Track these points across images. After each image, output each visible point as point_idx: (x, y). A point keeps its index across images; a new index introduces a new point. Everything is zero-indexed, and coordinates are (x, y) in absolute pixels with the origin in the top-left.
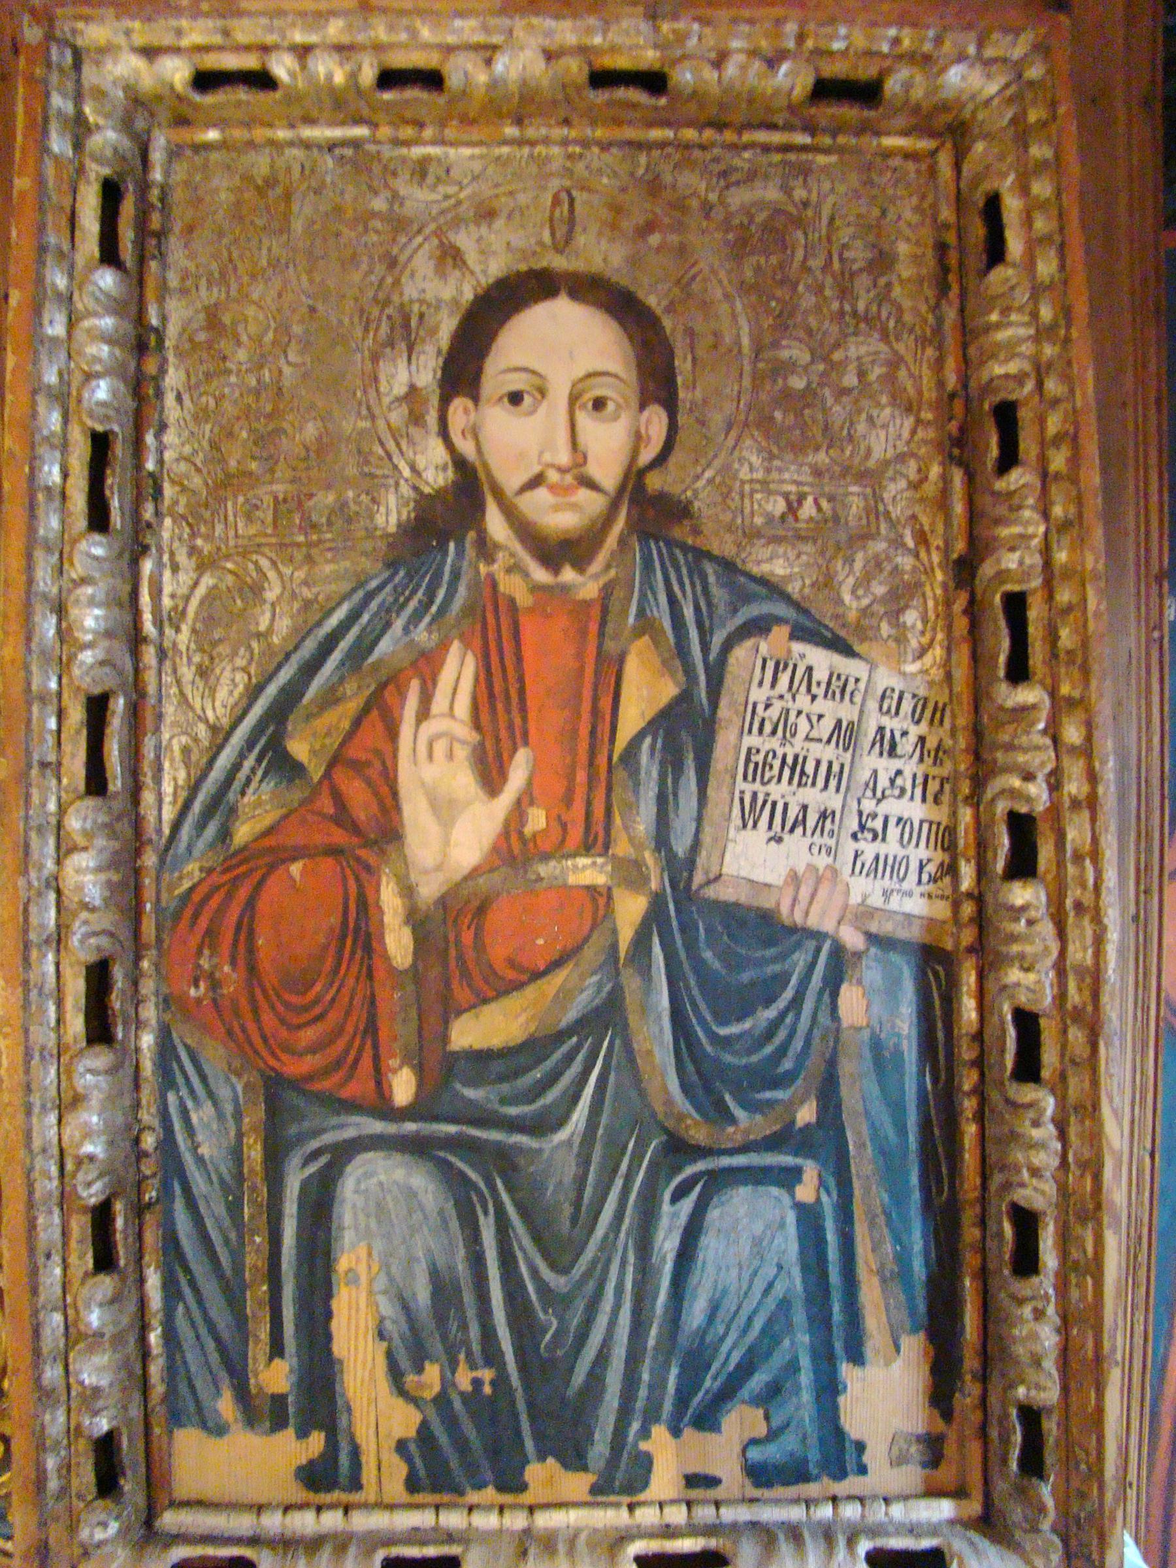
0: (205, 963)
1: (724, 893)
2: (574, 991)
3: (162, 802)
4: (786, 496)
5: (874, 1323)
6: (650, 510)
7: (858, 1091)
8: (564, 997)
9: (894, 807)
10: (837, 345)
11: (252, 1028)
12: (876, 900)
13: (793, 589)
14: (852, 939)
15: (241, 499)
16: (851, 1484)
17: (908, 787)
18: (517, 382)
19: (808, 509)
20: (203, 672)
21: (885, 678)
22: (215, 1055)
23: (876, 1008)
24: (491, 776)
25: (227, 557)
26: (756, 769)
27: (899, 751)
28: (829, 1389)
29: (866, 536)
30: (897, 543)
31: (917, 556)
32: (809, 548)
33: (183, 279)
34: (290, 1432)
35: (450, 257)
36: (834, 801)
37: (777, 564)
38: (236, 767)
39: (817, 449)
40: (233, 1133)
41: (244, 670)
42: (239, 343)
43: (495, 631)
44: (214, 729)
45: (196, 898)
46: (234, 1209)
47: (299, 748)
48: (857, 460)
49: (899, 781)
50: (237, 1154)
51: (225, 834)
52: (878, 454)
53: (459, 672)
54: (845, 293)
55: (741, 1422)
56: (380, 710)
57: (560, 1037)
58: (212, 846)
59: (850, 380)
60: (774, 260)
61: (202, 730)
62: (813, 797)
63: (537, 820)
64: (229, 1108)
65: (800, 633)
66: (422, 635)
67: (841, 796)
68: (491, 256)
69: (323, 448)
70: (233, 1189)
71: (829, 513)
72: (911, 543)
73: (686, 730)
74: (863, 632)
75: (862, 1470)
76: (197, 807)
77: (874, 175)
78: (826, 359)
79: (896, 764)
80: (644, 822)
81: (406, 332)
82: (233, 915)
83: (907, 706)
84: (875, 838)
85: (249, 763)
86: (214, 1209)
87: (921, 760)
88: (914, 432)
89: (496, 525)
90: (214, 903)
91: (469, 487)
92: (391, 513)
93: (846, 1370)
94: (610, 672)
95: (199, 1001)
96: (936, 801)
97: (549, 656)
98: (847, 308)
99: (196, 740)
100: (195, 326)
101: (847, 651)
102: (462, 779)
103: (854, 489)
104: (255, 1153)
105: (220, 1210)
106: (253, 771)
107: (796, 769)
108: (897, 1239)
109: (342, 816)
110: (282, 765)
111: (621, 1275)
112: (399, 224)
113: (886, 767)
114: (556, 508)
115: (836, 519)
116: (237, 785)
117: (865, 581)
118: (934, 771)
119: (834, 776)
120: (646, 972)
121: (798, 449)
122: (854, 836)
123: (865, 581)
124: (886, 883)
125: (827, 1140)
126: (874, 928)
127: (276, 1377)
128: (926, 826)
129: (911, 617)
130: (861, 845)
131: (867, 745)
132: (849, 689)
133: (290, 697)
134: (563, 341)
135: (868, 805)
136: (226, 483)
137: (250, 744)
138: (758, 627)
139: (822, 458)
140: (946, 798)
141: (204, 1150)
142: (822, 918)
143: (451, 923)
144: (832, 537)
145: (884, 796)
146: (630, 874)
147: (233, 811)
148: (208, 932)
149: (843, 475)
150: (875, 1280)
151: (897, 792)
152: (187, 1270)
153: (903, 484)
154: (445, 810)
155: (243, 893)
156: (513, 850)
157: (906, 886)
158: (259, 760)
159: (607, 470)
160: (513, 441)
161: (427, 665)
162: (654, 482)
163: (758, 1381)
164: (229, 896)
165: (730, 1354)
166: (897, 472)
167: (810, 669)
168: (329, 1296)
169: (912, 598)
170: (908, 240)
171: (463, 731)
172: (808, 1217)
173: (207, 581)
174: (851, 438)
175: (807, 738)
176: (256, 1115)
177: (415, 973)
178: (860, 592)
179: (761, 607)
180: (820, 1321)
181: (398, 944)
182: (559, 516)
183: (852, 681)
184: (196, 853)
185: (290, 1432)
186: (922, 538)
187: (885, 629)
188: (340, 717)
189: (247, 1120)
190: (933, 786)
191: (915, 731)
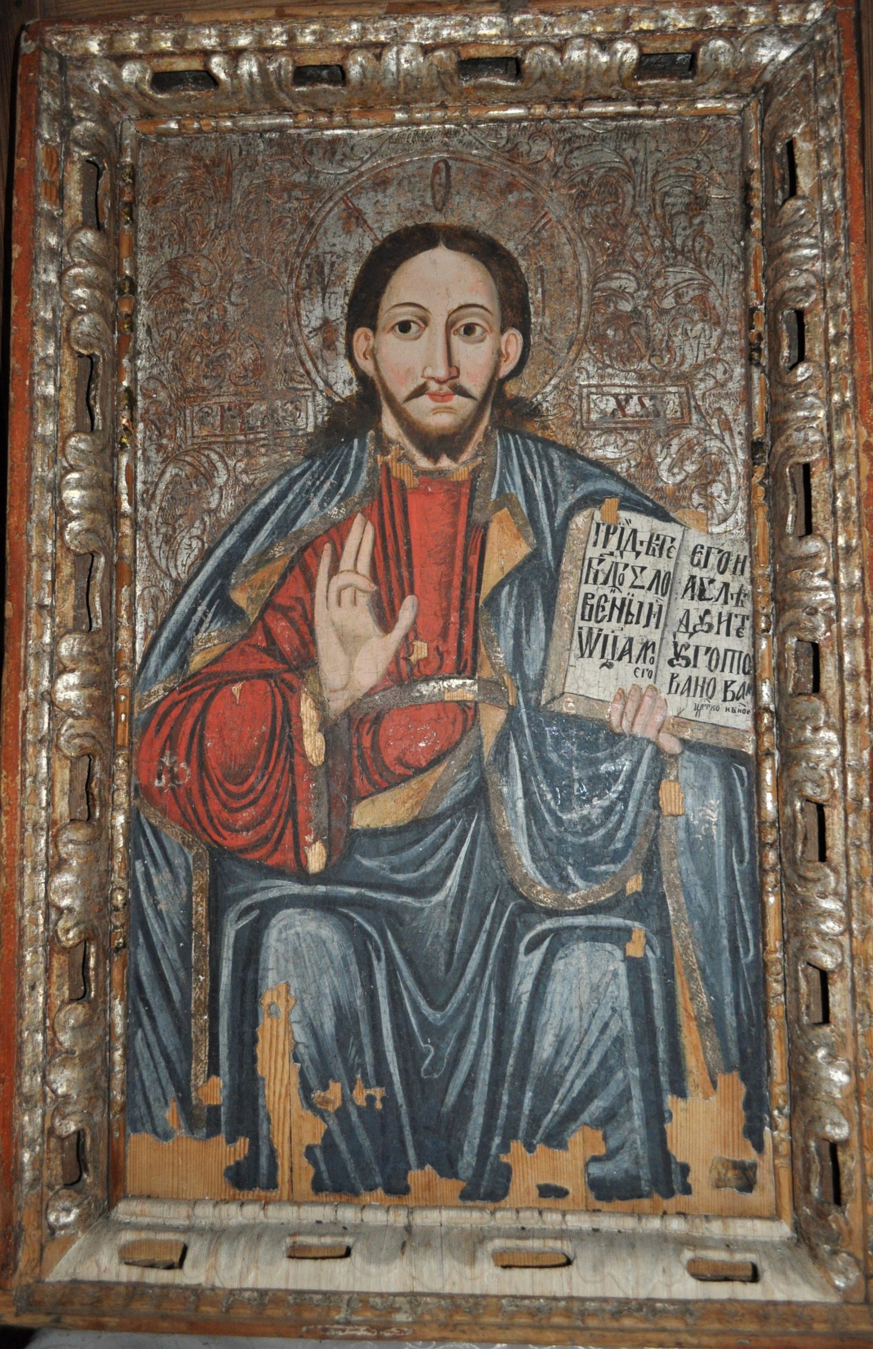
0: (167, 761)
1: (569, 707)
2: (450, 781)
3: (135, 637)
4: (616, 396)
5: (694, 1063)
6: (507, 409)
7: (676, 867)
8: (440, 790)
9: (703, 639)
10: (658, 275)
11: (201, 810)
12: (690, 714)
13: (621, 468)
14: (671, 745)
15: (197, 409)
16: (679, 1200)
17: (715, 623)
18: (406, 313)
19: (633, 407)
20: (168, 540)
21: (695, 538)
22: (173, 834)
23: (696, 804)
24: (385, 619)
25: (186, 453)
26: (592, 610)
27: (707, 595)
28: (657, 1118)
29: (681, 425)
30: (707, 431)
31: (722, 441)
32: (635, 437)
33: (151, 240)
34: (222, 1138)
35: (354, 218)
36: (654, 635)
37: (608, 451)
38: (193, 611)
39: (641, 359)
40: (184, 893)
41: (199, 538)
42: (194, 289)
43: (388, 506)
44: (176, 582)
45: (161, 710)
46: (184, 954)
47: (239, 598)
48: (674, 365)
49: (707, 619)
50: (188, 909)
51: (184, 661)
52: (690, 361)
53: (361, 538)
54: (666, 233)
55: (582, 1142)
56: (302, 567)
57: (439, 819)
58: (173, 672)
59: (669, 302)
60: (608, 209)
61: (167, 584)
62: (636, 631)
63: (421, 650)
64: (182, 874)
65: (626, 504)
66: (334, 511)
67: (660, 631)
68: (388, 215)
69: (259, 368)
70: (183, 937)
71: (651, 409)
72: (717, 431)
73: (538, 580)
74: (677, 502)
75: (687, 1190)
76: (162, 642)
77: (692, 135)
78: (650, 286)
79: (705, 605)
80: (502, 653)
81: (320, 279)
82: (189, 722)
83: (713, 560)
84: (687, 665)
85: (201, 609)
86: (170, 954)
87: (726, 602)
88: (720, 342)
89: (390, 425)
90: (175, 713)
91: (370, 395)
92: (310, 417)
93: (670, 1100)
94: (477, 540)
95: (161, 789)
96: (738, 635)
98: (668, 244)
99: (162, 591)
100: (160, 275)
101: (665, 517)
102: (363, 619)
103: (673, 389)
104: (201, 909)
105: (173, 954)
106: (205, 614)
107: (623, 610)
108: (711, 990)
109: (272, 646)
110: (227, 610)
111: (485, 1013)
112: (316, 193)
113: (696, 608)
114: (436, 411)
115: (657, 415)
116: (192, 625)
117: (679, 462)
118: (736, 611)
119: (654, 615)
120: (505, 769)
121: (625, 359)
122: (671, 663)
123: (679, 462)
124: (697, 700)
125: (649, 905)
126: (687, 735)
127: (214, 1091)
128: (730, 654)
129: (717, 489)
130: (677, 670)
131: (681, 591)
132: (666, 547)
133: (233, 559)
135: (682, 638)
136: (186, 397)
137: (203, 593)
138: (593, 500)
139: (645, 365)
140: (747, 632)
141: (162, 906)
142: (643, 727)
143: (356, 729)
144: (653, 428)
145: (695, 631)
146: (492, 689)
147: (189, 644)
148: (169, 737)
149: (663, 379)
150: (693, 1024)
151: (705, 628)
152: (146, 1003)
153: (711, 383)
154: (349, 642)
155: (197, 706)
156: (402, 674)
157: (713, 702)
158: (209, 606)
159: (475, 381)
160: (403, 360)
161: (337, 533)
162: (512, 389)
163: (597, 1106)
164: (185, 711)
165: (574, 1083)
166: (707, 374)
167: (634, 531)
168: (255, 1024)
169: (718, 474)
170: (719, 186)
171: (364, 583)
172: (636, 968)
173: (171, 471)
174: (669, 349)
175: (633, 586)
176: (201, 879)
177: (328, 768)
178: (676, 470)
180: (649, 1060)
181: (313, 746)
183: (668, 540)
184: (161, 677)
185: (222, 1138)
186: (726, 425)
187: (696, 499)
188: (270, 574)
189: (195, 883)
190: (736, 623)
191: (720, 579)
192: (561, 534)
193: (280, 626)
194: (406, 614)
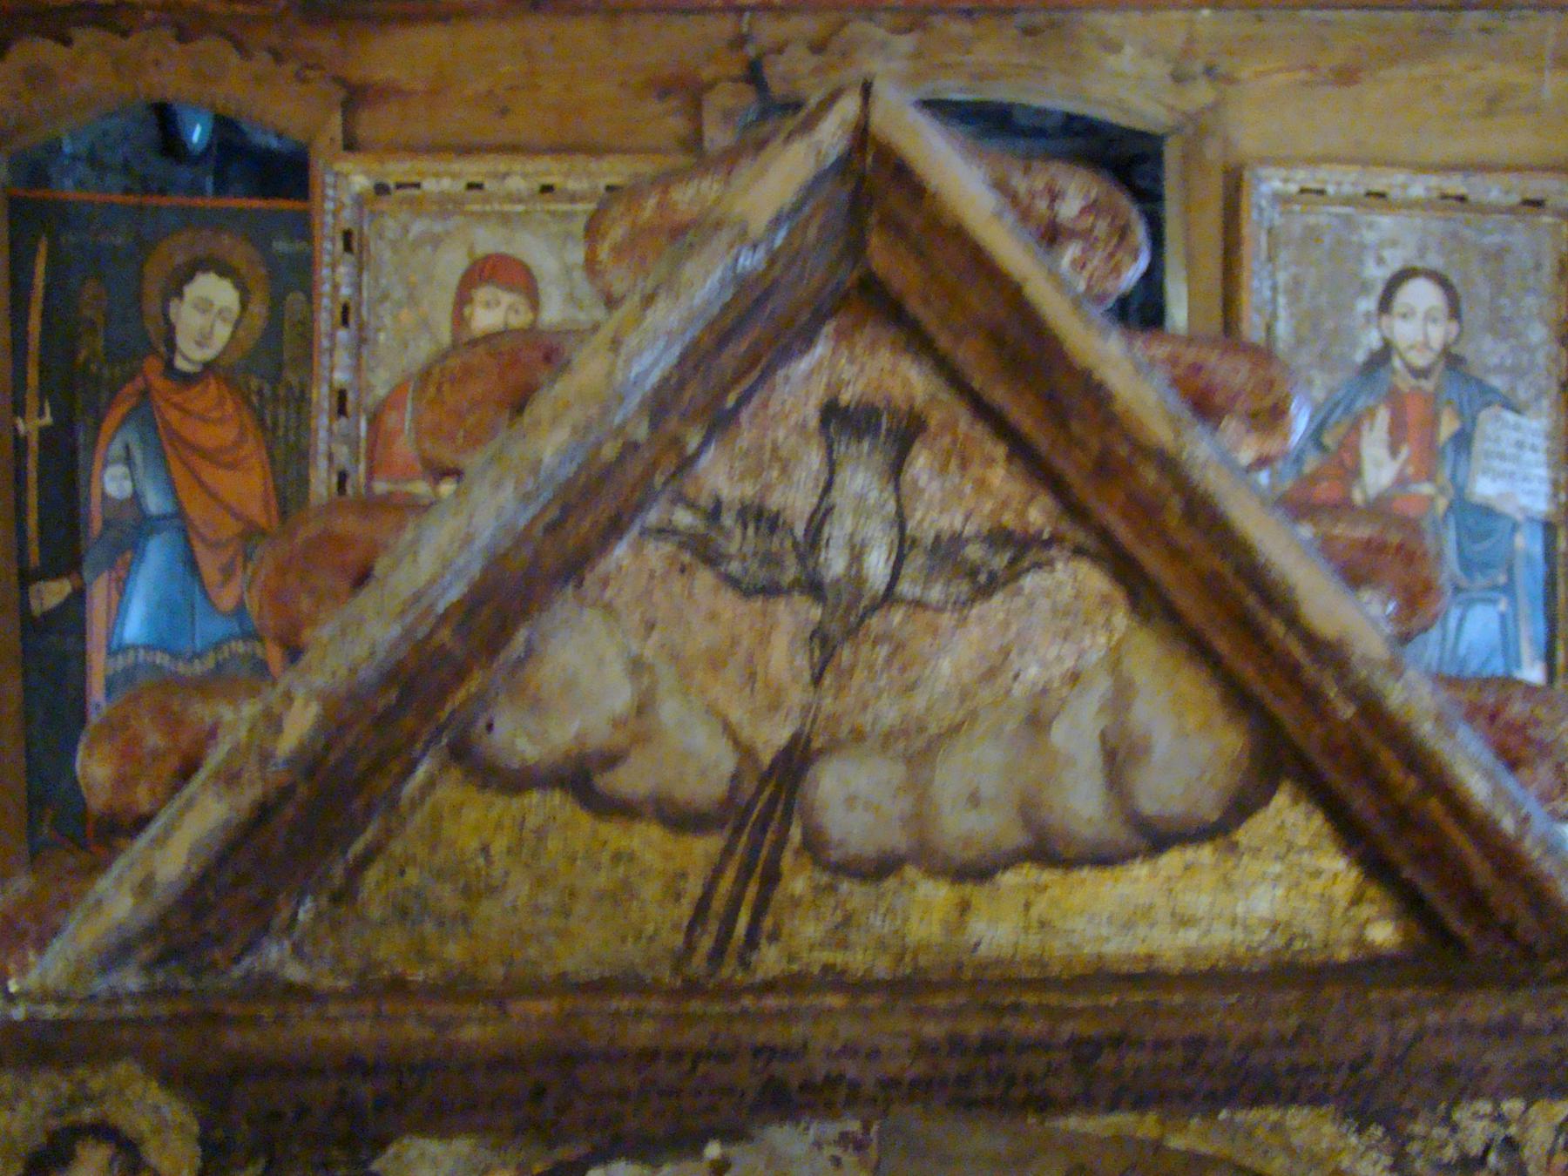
6: (1452, 360)
7: (1521, 574)
14: (1519, 517)
18: (1403, 310)
26: (1487, 455)
35: (1380, 261)
37: (1497, 381)
43: (1395, 399)
53: (1383, 417)
56: (1356, 427)
66: (1371, 402)
68: (1396, 260)
73: (1463, 440)
81: (1365, 288)
89: (1397, 362)
92: (1360, 357)
97: (1415, 412)
107: (1502, 457)
109: (1341, 463)
110: (1320, 446)
112: (1363, 247)
125: (1508, 589)
134: (1421, 295)
138: (1488, 404)
144: (1516, 372)
146: (1442, 491)
156: (1401, 481)
160: (1405, 332)
161: (1371, 413)
162: (1454, 350)
172: (1503, 617)
179: (1487, 396)
182: (1420, 360)
188: (1341, 430)
192: (1474, 419)
193: (1346, 456)
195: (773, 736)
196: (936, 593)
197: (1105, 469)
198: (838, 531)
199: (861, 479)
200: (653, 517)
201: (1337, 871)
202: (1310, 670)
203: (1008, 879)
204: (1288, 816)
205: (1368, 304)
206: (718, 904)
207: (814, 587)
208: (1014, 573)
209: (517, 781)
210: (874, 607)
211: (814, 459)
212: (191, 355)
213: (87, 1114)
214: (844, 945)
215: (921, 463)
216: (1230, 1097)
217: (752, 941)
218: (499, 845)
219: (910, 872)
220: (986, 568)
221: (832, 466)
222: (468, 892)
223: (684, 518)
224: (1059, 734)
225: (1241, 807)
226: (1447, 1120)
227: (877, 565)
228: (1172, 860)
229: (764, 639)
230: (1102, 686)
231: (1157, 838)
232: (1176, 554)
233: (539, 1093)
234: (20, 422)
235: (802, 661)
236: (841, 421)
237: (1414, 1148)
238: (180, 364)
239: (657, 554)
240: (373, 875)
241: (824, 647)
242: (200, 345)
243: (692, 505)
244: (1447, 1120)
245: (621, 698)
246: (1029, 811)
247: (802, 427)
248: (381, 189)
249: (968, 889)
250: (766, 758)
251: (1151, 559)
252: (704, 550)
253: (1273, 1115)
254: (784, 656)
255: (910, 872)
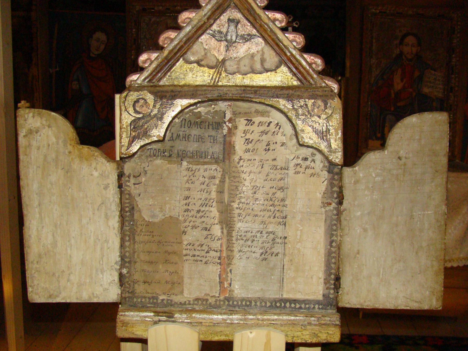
14: (434, 98)
24: (402, 81)
89: (404, 57)
92: (394, 56)
107: (430, 82)
134: (410, 40)
160: (406, 49)
181: (393, 96)
182: (409, 57)
194: (405, 81)
195: (221, 58)
196: (241, 42)
197: (261, 26)
198: (229, 34)
199: (232, 28)
200: (207, 32)
201: (289, 75)
202: (285, 50)
203: (249, 75)
204: (284, 69)
205: (397, 42)
206: (214, 78)
207: (226, 40)
208: (250, 39)
209: (191, 63)
210: (233, 43)
211: (227, 25)
212: (94, 52)
213: (141, 97)
214: (229, 82)
215: (239, 26)
216: (273, 97)
217: (218, 82)
218: (188, 70)
219: (237, 74)
220: (248, 38)
221: (229, 26)
222: (184, 75)
223: (211, 32)
224: (255, 58)
225: (278, 67)
226: (299, 101)
227: (234, 38)
228: (269, 73)
229: (220, 46)
230: (261, 52)
231: (267, 71)
232: (270, 36)
233: (193, 94)
234: (51, 70)
235: (225, 49)
236: (230, 20)
237: (294, 104)
238: (92, 55)
239: (208, 36)
240: (173, 73)
241: (227, 49)
242: (97, 50)
243: (212, 30)
244: (299, 101)
245: (203, 53)
246: (251, 68)
247: (225, 22)
248: (144, 10)
249: (244, 76)
250: (220, 61)
251: (266, 36)
252: (214, 36)
253: (278, 99)
254: (223, 49)
255: (237, 74)
